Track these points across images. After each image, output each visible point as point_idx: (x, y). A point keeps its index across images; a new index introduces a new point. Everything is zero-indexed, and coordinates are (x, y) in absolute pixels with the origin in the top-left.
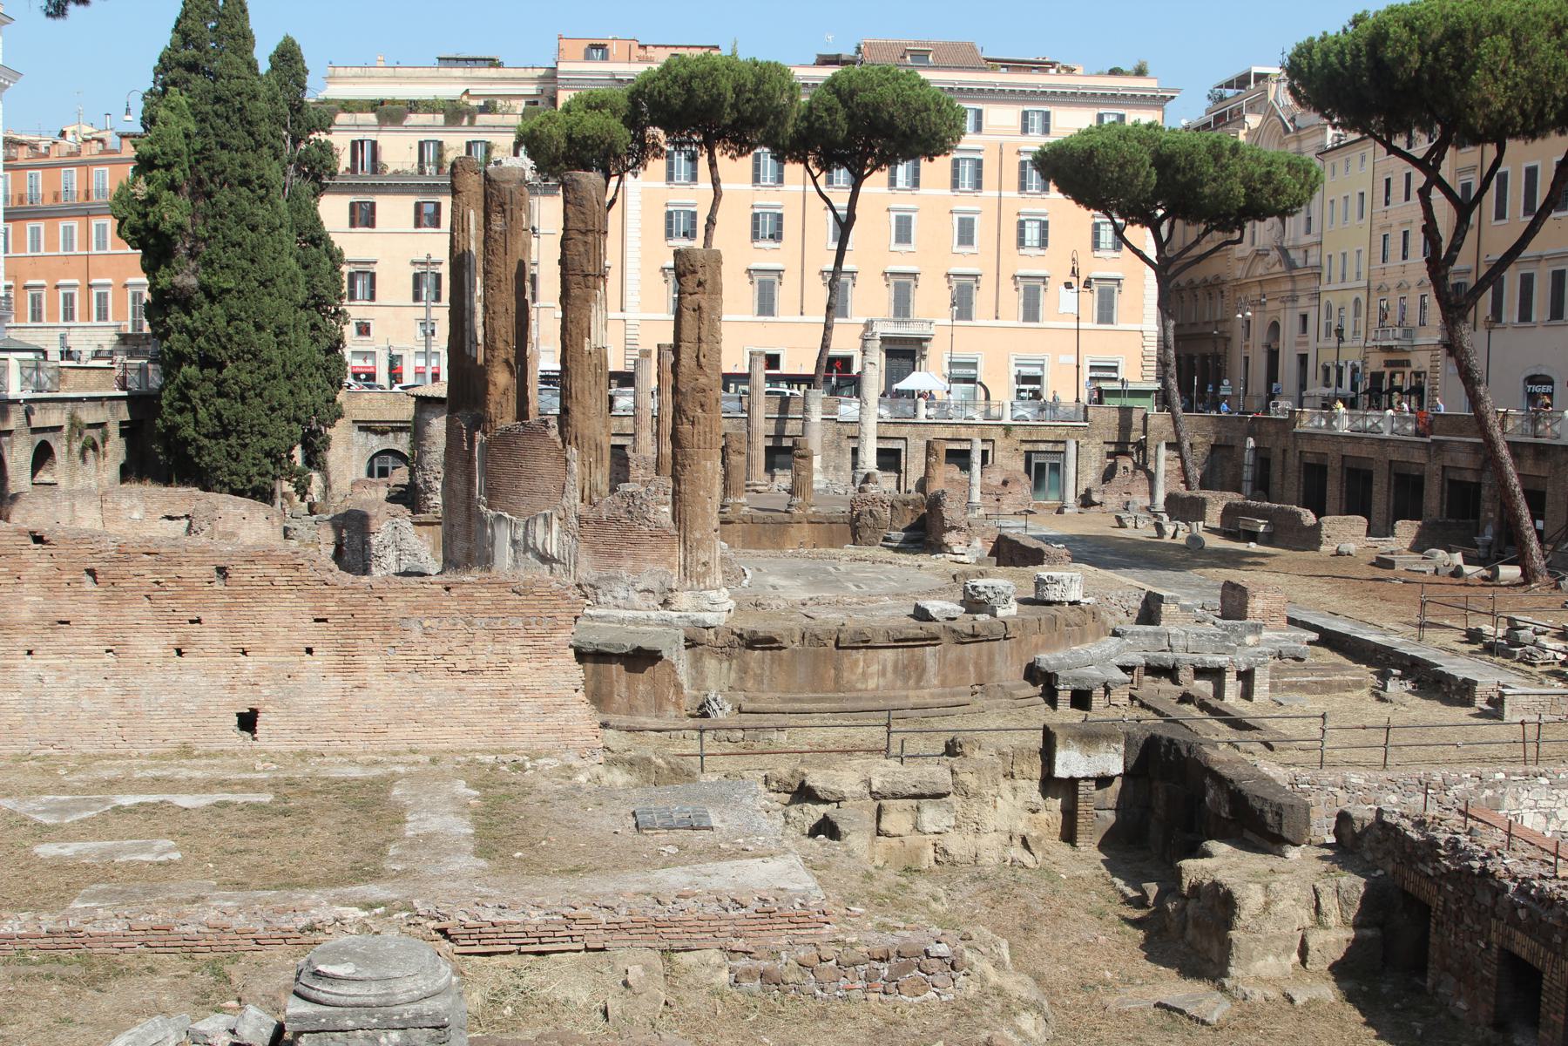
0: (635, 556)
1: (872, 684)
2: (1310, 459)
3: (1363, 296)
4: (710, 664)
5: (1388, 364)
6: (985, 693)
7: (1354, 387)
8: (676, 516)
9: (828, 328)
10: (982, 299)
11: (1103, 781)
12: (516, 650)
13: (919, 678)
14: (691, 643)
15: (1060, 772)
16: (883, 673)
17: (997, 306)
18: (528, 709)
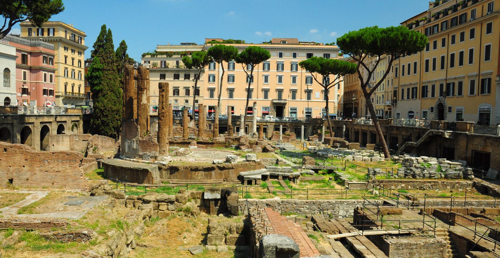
0: (150, 149)
1: (199, 178)
2: (356, 130)
3: (384, 94)
4: (164, 172)
5: (389, 109)
6: (227, 181)
7: (382, 114)
8: (158, 141)
9: (248, 100)
10: (298, 95)
11: (216, 200)
12: (68, 167)
13: (210, 177)
14: (160, 169)
15: (206, 197)
16: (202, 175)
17: (301, 96)
18: (70, 179)
